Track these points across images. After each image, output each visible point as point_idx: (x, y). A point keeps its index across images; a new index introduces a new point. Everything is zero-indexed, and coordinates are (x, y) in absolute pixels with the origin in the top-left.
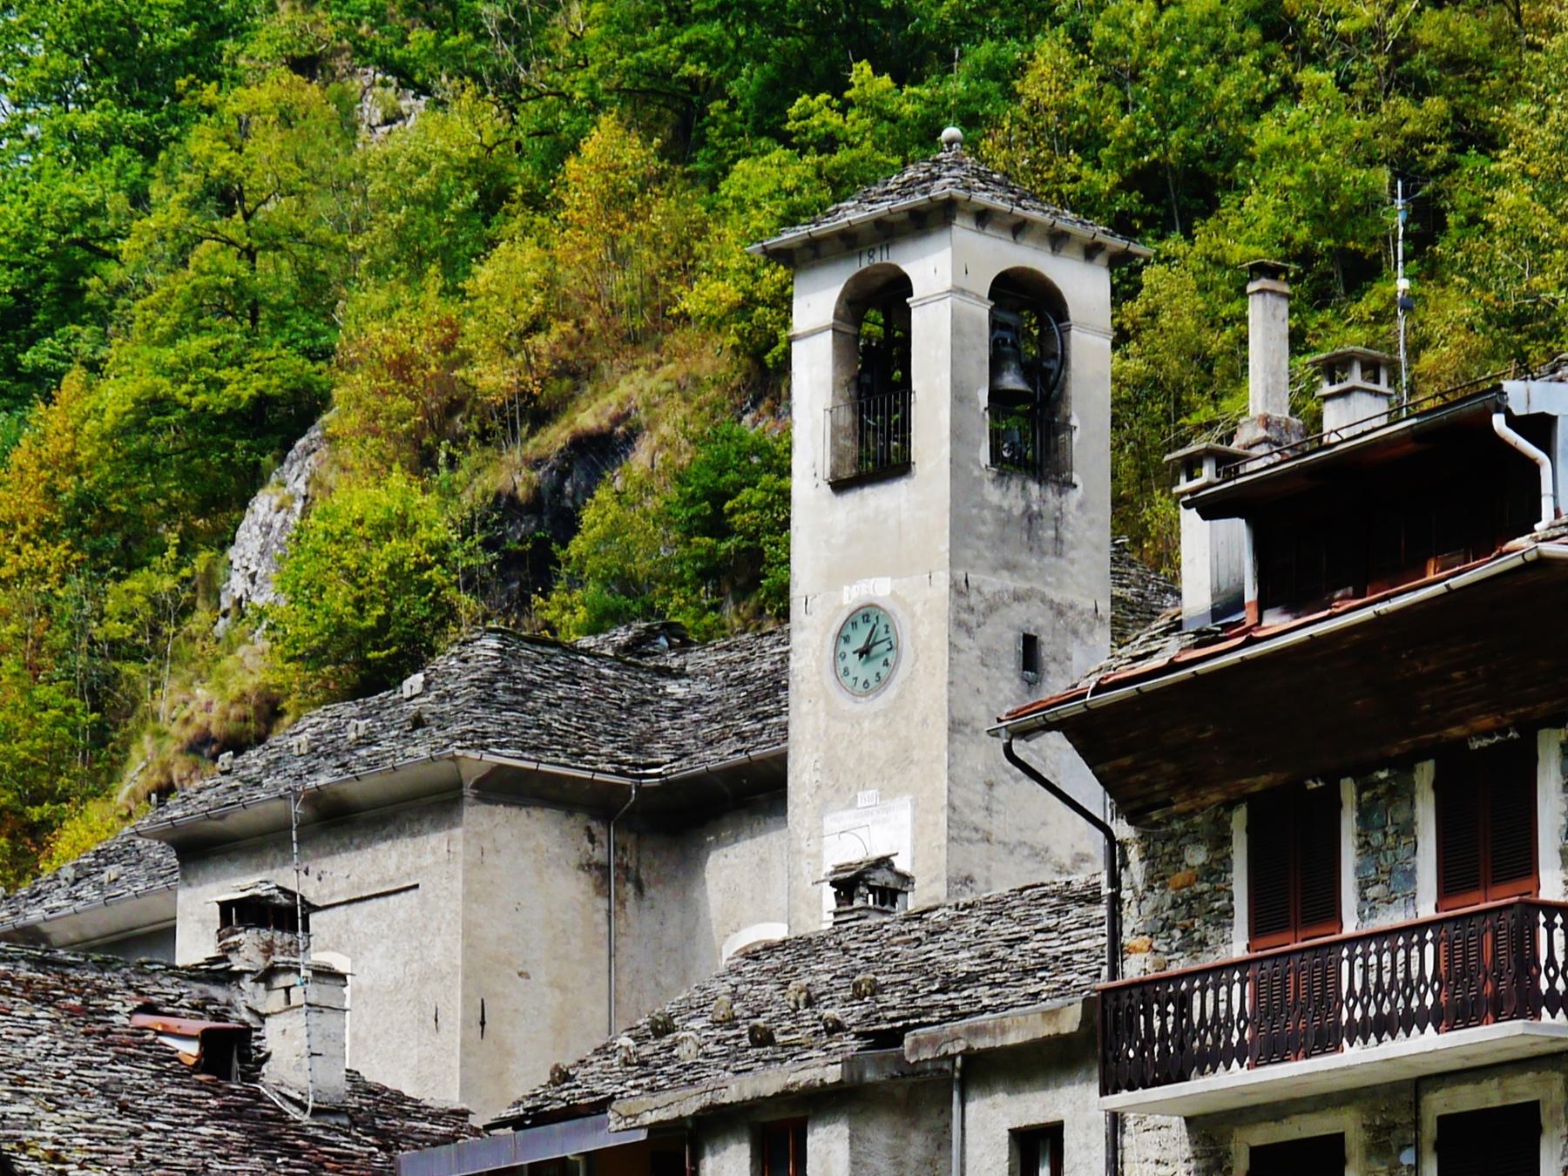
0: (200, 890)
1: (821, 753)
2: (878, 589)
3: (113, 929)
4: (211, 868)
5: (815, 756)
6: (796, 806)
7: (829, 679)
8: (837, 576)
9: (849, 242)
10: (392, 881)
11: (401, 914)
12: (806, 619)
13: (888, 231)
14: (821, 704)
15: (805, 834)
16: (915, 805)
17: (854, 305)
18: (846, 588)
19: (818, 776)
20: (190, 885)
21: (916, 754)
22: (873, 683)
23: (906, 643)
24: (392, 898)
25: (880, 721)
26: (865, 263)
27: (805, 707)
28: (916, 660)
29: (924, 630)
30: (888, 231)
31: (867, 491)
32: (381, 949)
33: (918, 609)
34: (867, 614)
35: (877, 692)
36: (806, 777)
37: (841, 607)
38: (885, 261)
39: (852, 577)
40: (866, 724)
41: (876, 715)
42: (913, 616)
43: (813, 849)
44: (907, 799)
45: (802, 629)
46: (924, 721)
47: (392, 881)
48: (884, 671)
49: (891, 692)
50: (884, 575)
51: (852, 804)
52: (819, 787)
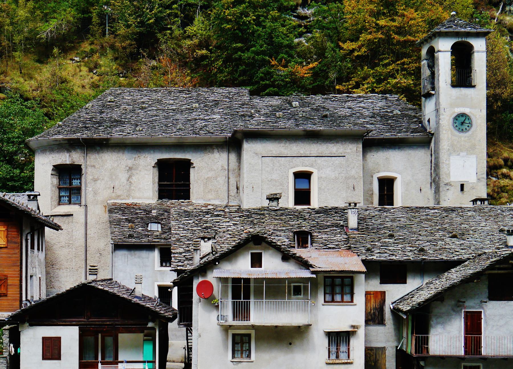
0: (253, 146)
1: (450, 143)
2: (467, 111)
3: (138, 142)
4: (258, 141)
5: (448, 143)
6: (442, 153)
7: (452, 127)
8: (452, 105)
9: (457, 34)
10: (335, 154)
11: (337, 162)
12: (444, 113)
13: (469, 35)
14: (449, 132)
15: (445, 159)
16: (477, 158)
17: (455, 49)
18: (456, 109)
19: (449, 147)
20: (249, 144)
21: (477, 147)
22: (464, 129)
23: (474, 123)
24: (333, 158)
25: (467, 138)
26: (460, 40)
27: (444, 132)
28: (477, 127)
29: (479, 121)
30: (469, 35)
31: (462, 89)
32: (329, 169)
33: (477, 116)
34: (463, 115)
35: (466, 132)
36: (445, 147)
37: (454, 112)
38: (466, 40)
39: (458, 106)
40: (463, 139)
41: (465, 137)
42: (476, 118)
43: (447, 163)
44: (475, 156)
45: (443, 115)
46: (480, 140)
47: (335, 154)
48: (468, 128)
49: (470, 133)
50: (468, 108)
51: (459, 155)
52: (449, 150)
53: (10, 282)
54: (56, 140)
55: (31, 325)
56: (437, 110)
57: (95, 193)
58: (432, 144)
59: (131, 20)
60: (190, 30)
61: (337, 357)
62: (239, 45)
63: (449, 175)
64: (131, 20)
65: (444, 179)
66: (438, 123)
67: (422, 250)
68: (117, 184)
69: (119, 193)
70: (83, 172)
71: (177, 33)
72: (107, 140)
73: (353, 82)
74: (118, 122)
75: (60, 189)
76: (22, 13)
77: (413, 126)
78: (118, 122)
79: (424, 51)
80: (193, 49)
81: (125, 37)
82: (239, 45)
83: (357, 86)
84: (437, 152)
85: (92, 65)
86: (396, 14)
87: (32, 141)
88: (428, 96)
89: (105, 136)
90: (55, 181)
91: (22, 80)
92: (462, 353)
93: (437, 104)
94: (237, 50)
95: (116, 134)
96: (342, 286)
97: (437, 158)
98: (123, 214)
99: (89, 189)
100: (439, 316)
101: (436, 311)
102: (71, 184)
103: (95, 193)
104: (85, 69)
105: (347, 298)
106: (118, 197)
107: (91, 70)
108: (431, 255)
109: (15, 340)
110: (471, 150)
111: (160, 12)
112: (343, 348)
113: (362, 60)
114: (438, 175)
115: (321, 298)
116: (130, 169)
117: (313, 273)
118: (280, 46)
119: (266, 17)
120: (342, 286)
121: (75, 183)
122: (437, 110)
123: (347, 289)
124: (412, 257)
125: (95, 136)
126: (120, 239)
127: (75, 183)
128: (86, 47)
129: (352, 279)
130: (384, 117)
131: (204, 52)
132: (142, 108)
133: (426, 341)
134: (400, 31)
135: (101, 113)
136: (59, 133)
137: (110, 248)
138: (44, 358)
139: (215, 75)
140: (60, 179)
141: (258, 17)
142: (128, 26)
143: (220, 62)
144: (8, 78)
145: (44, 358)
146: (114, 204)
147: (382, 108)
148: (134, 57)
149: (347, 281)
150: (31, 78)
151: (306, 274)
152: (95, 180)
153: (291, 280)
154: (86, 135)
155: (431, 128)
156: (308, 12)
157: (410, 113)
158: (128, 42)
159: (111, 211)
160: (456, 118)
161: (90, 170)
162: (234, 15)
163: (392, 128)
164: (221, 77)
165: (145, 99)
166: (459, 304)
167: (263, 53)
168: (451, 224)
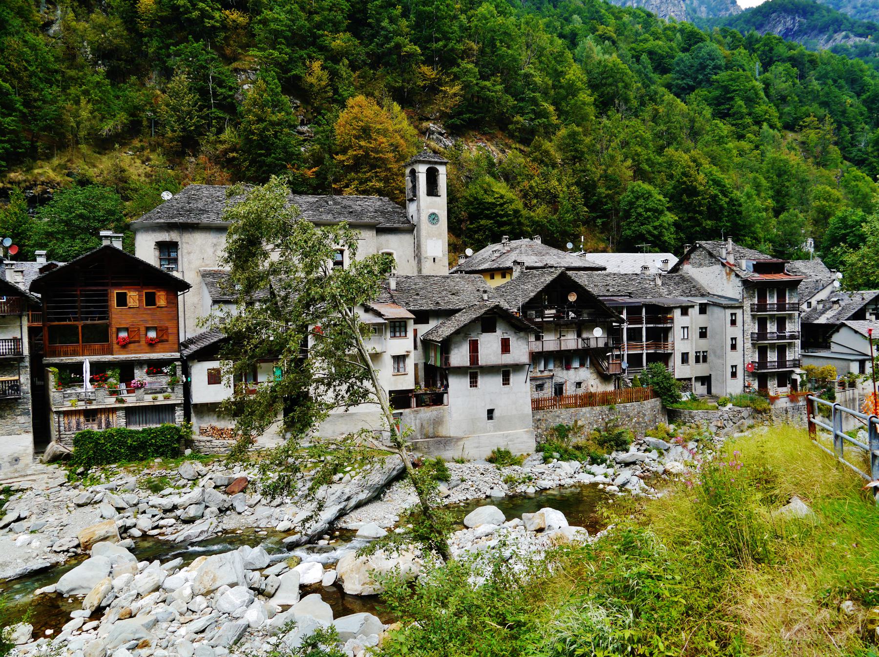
53: (170, 331)
54: (158, 223)
55: (199, 361)
56: (418, 210)
57: (190, 263)
58: (415, 232)
59: (176, 127)
60: (223, 137)
61: (398, 371)
62: (263, 152)
63: (426, 252)
64: (176, 127)
65: (424, 255)
66: (419, 218)
67: (438, 303)
68: (205, 256)
69: (207, 262)
70: (180, 246)
71: (212, 138)
72: (198, 224)
73: (343, 183)
74: (203, 211)
75: (161, 259)
76: (85, 114)
77: (401, 219)
78: (203, 211)
79: (408, 171)
80: (225, 152)
81: (172, 140)
82: (263, 152)
83: (347, 186)
84: (418, 236)
85: (144, 158)
86: (371, 137)
87: (136, 221)
88: (411, 200)
89: (196, 221)
90: (157, 253)
91: (86, 167)
92: (468, 364)
93: (418, 206)
94: (261, 155)
95: (205, 220)
96: (400, 327)
97: (419, 241)
98: (214, 278)
99: (185, 260)
100: (455, 343)
101: (454, 340)
102: (169, 255)
103: (190, 263)
104: (138, 162)
105: (403, 334)
106: (207, 265)
107: (143, 162)
108: (443, 306)
109: (186, 372)
110: (439, 236)
111: (198, 121)
112: (401, 365)
113: (349, 169)
114: (419, 251)
115: (389, 335)
116: (215, 245)
117: (385, 319)
118: (293, 154)
119: (281, 133)
120: (400, 327)
121: (173, 255)
122: (418, 210)
123: (403, 329)
124: (432, 307)
125: (189, 221)
126: (217, 296)
127: (173, 255)
128: (136, 143)
129: (405, 322)
130: (383, 213)
131: (235, 154)
132: (219, 201)
133: (447, 359)
134: (375, 150)
135: (189, 203)
136: (160, 218)
137: (211, 302)
138: (209, 383)
139: (244, 172)
140: (160, 252)
141: (276, 132)
142: (174, 131)
143: (247, 163)
144: (74, 166)
145: (209, 383)
146: (205, 271)
147: (380, 206)
148: (182, 154)
149: (403, 324)
150: (94, 166)
151: (380, 320)
152: (189, 253)
153: (374, 324)
154: (181, 220)
155: (415, 221)
156: (305, 129)
157: (398, 210)
158: (175, 143)
159: (203, 276)
160: (430, 216)
161: (185, 245)
162: (258, 129)
163: (389, 221)
164: (248, 174)
165: (219, 194)
166: (466, 336)
167: (280, 159)
168: (449, 286)
